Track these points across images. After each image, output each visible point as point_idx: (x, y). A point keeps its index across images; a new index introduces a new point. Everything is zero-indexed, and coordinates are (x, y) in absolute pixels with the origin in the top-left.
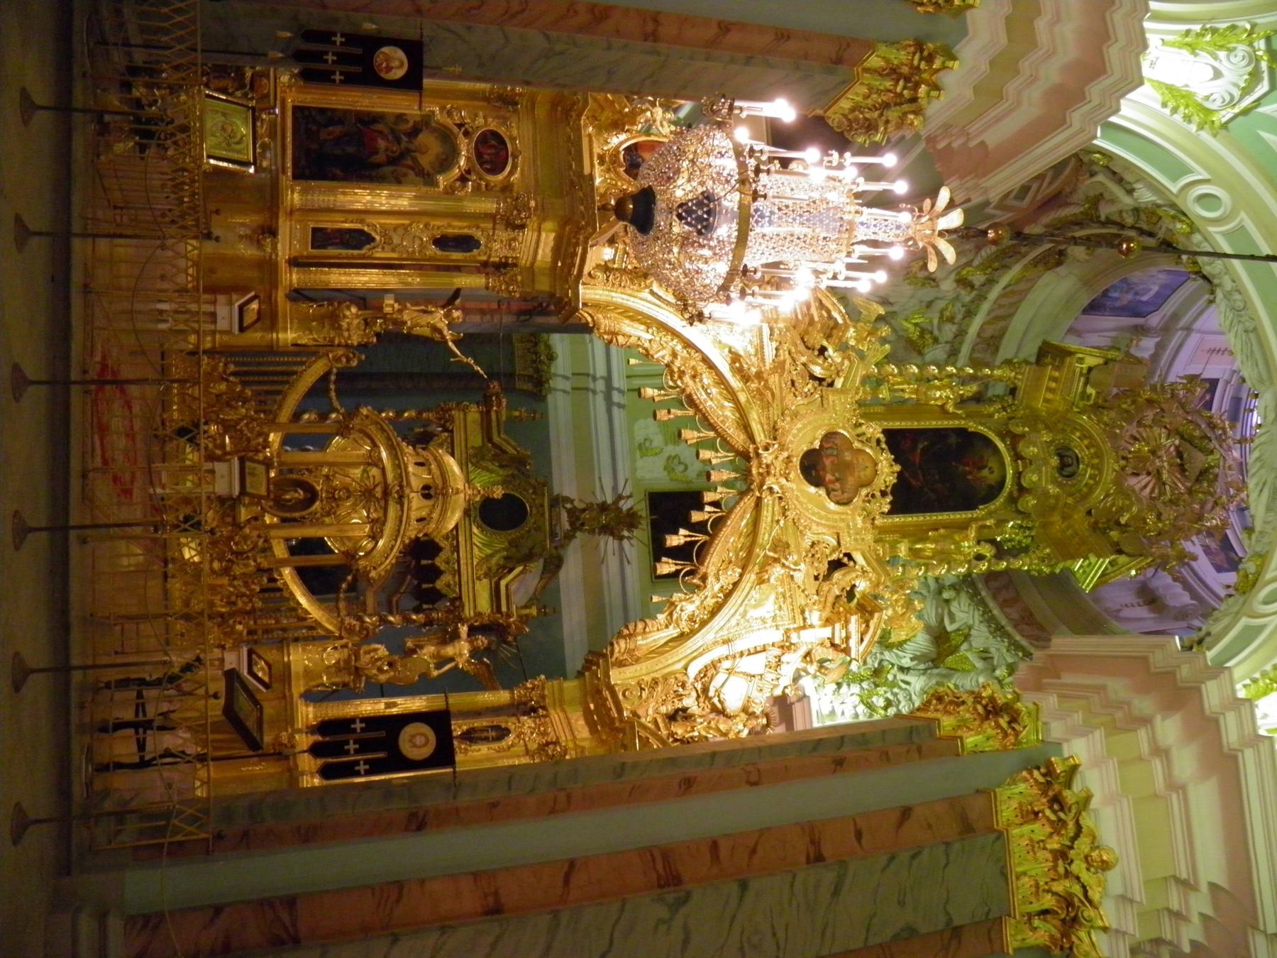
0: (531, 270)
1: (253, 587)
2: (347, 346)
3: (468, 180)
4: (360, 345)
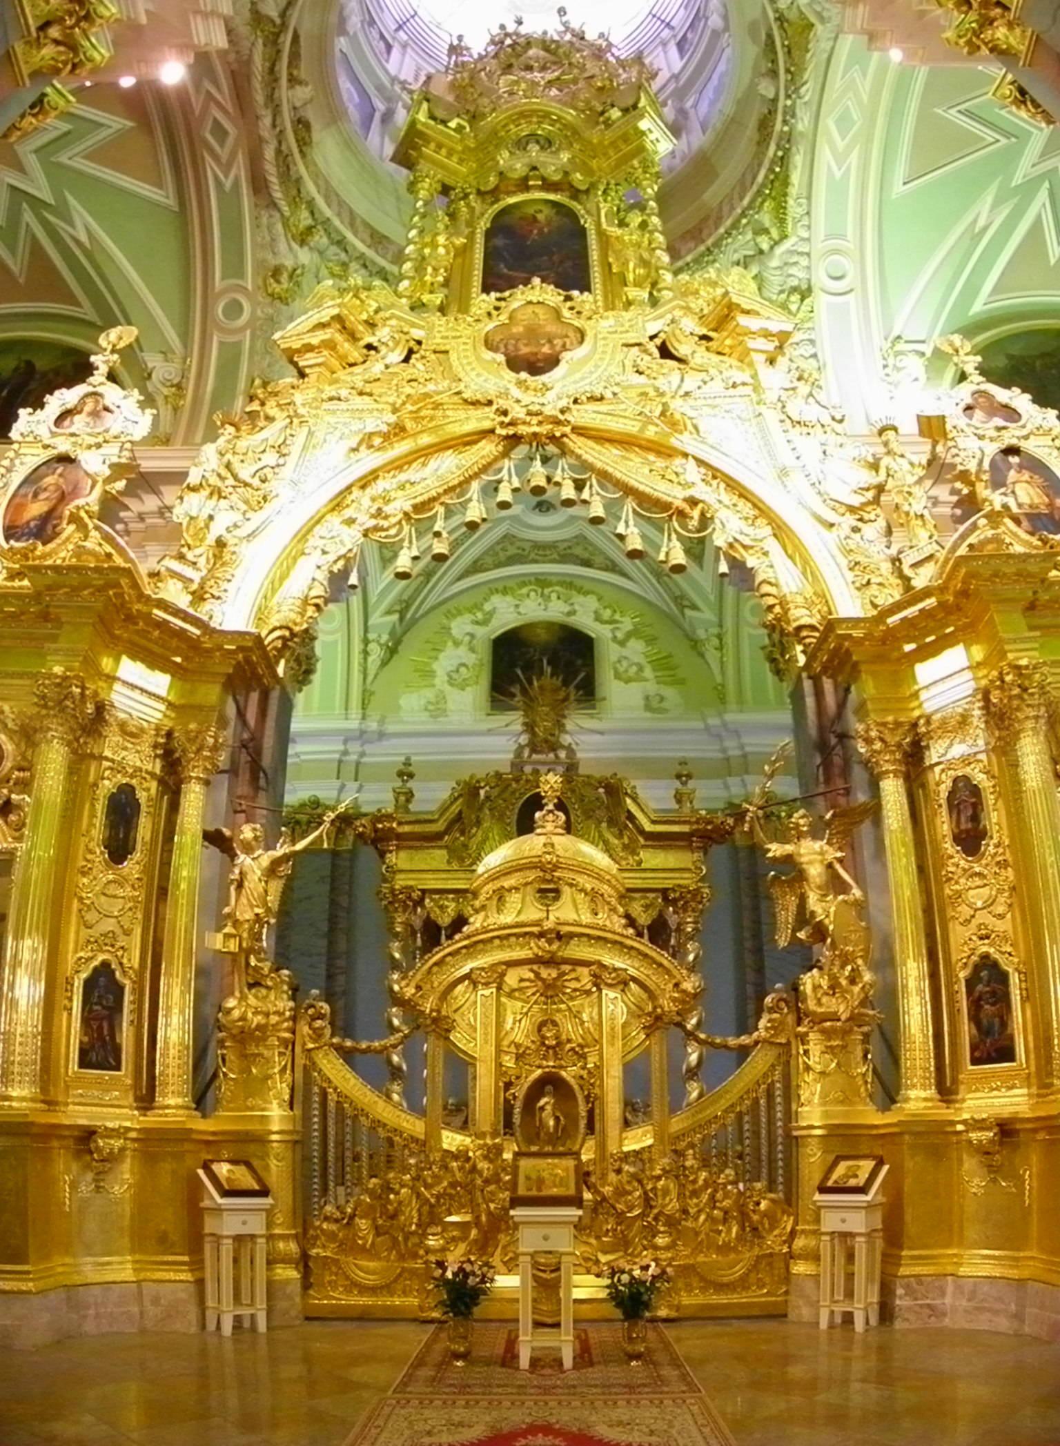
2: (294, 1019)
4: (293, 998)
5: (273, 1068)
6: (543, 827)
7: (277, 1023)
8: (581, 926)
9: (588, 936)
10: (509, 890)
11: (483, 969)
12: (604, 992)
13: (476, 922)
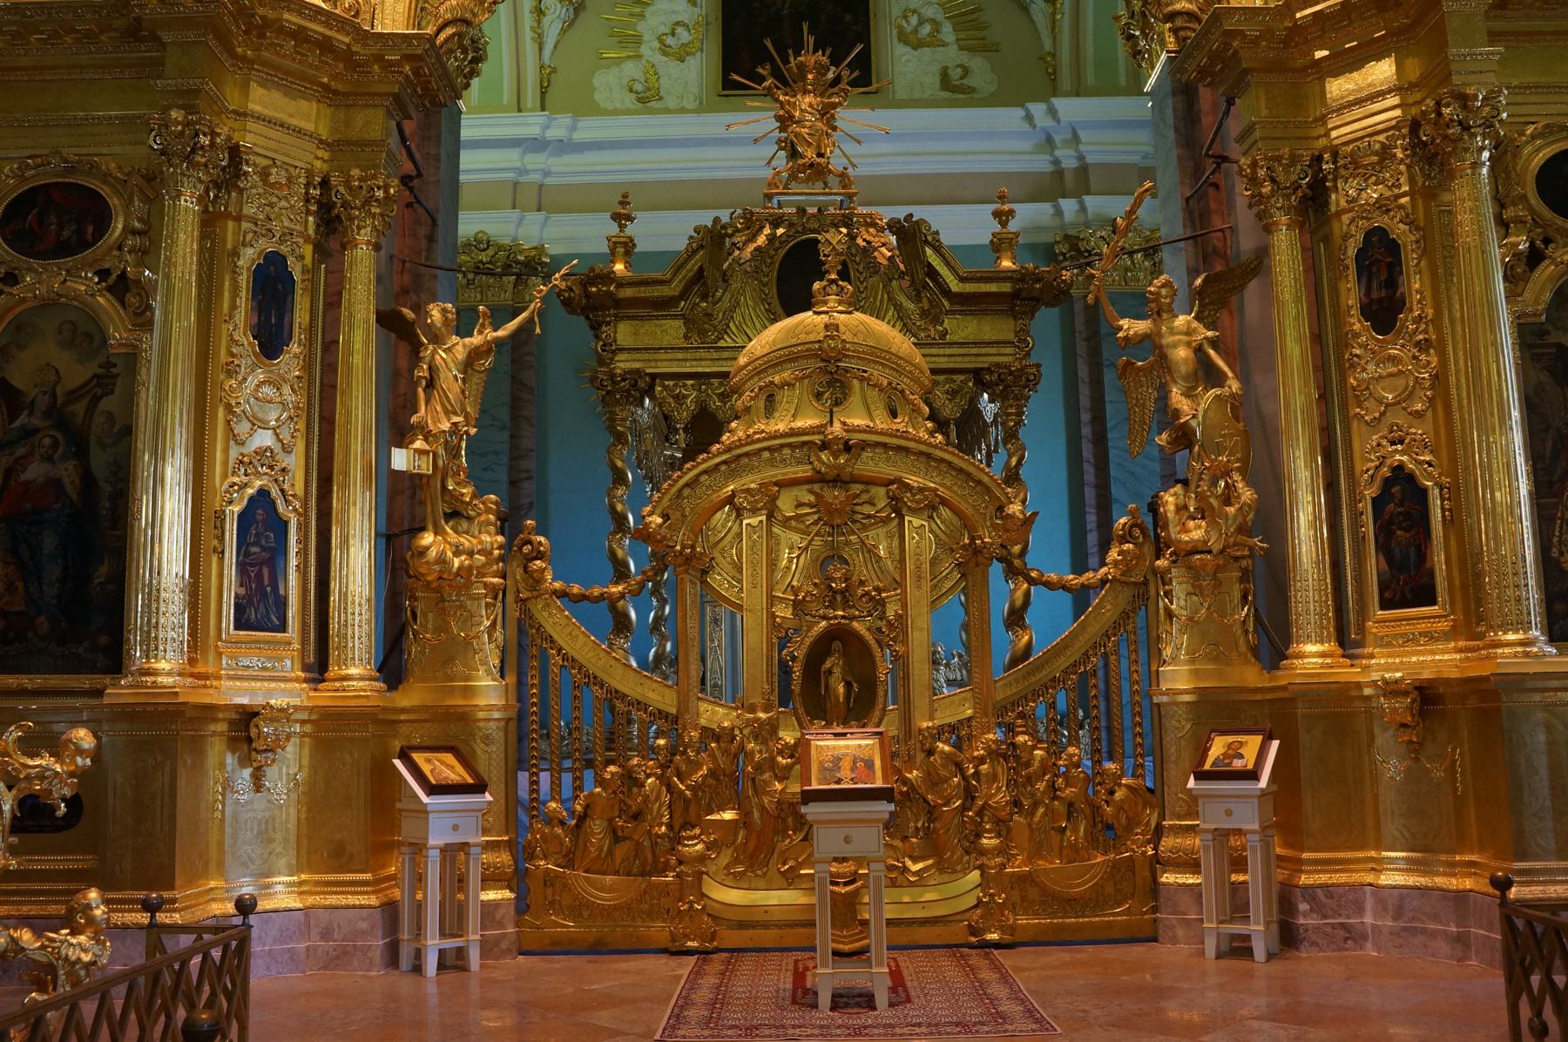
0: (338, 147)
1: (1036, 764)
3: (123, 276)
5: (479, 624)
6: (825, 303)
7: (484, 565)
8: (876, 433)
9: (885, 446)
10: (781, 386)
11: (748, 491)
12: (907, 518)
13: (737, 431)
